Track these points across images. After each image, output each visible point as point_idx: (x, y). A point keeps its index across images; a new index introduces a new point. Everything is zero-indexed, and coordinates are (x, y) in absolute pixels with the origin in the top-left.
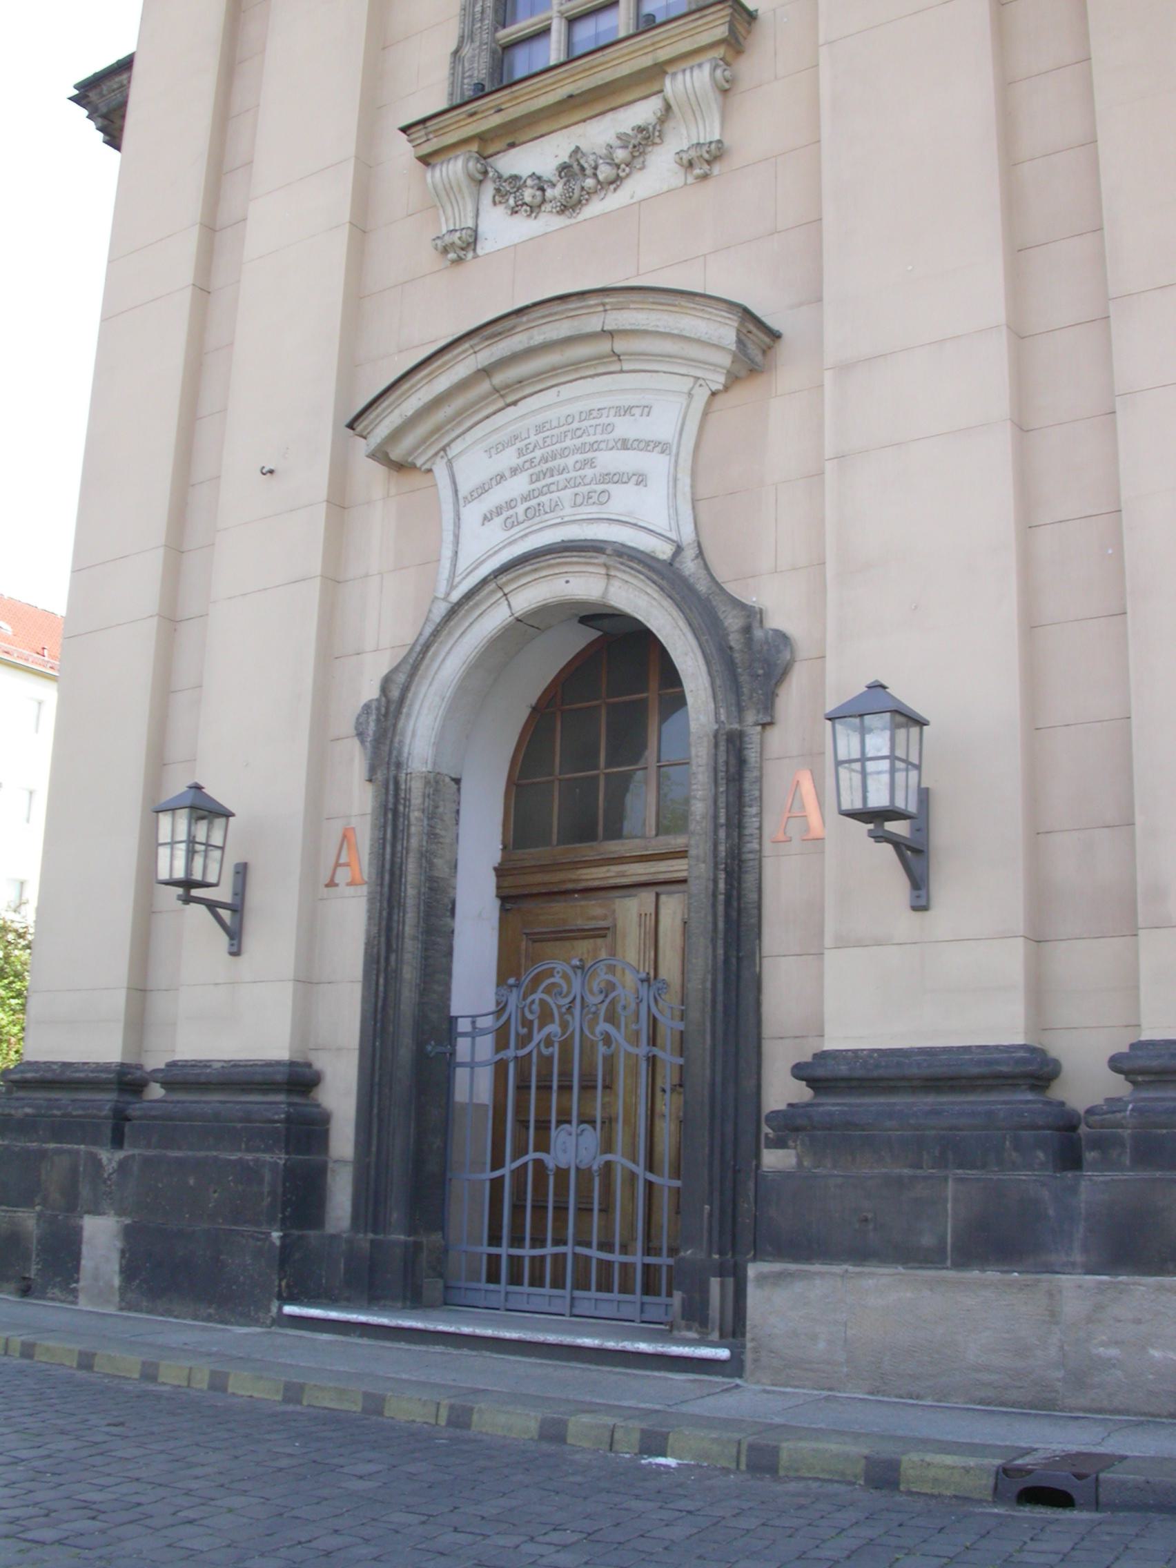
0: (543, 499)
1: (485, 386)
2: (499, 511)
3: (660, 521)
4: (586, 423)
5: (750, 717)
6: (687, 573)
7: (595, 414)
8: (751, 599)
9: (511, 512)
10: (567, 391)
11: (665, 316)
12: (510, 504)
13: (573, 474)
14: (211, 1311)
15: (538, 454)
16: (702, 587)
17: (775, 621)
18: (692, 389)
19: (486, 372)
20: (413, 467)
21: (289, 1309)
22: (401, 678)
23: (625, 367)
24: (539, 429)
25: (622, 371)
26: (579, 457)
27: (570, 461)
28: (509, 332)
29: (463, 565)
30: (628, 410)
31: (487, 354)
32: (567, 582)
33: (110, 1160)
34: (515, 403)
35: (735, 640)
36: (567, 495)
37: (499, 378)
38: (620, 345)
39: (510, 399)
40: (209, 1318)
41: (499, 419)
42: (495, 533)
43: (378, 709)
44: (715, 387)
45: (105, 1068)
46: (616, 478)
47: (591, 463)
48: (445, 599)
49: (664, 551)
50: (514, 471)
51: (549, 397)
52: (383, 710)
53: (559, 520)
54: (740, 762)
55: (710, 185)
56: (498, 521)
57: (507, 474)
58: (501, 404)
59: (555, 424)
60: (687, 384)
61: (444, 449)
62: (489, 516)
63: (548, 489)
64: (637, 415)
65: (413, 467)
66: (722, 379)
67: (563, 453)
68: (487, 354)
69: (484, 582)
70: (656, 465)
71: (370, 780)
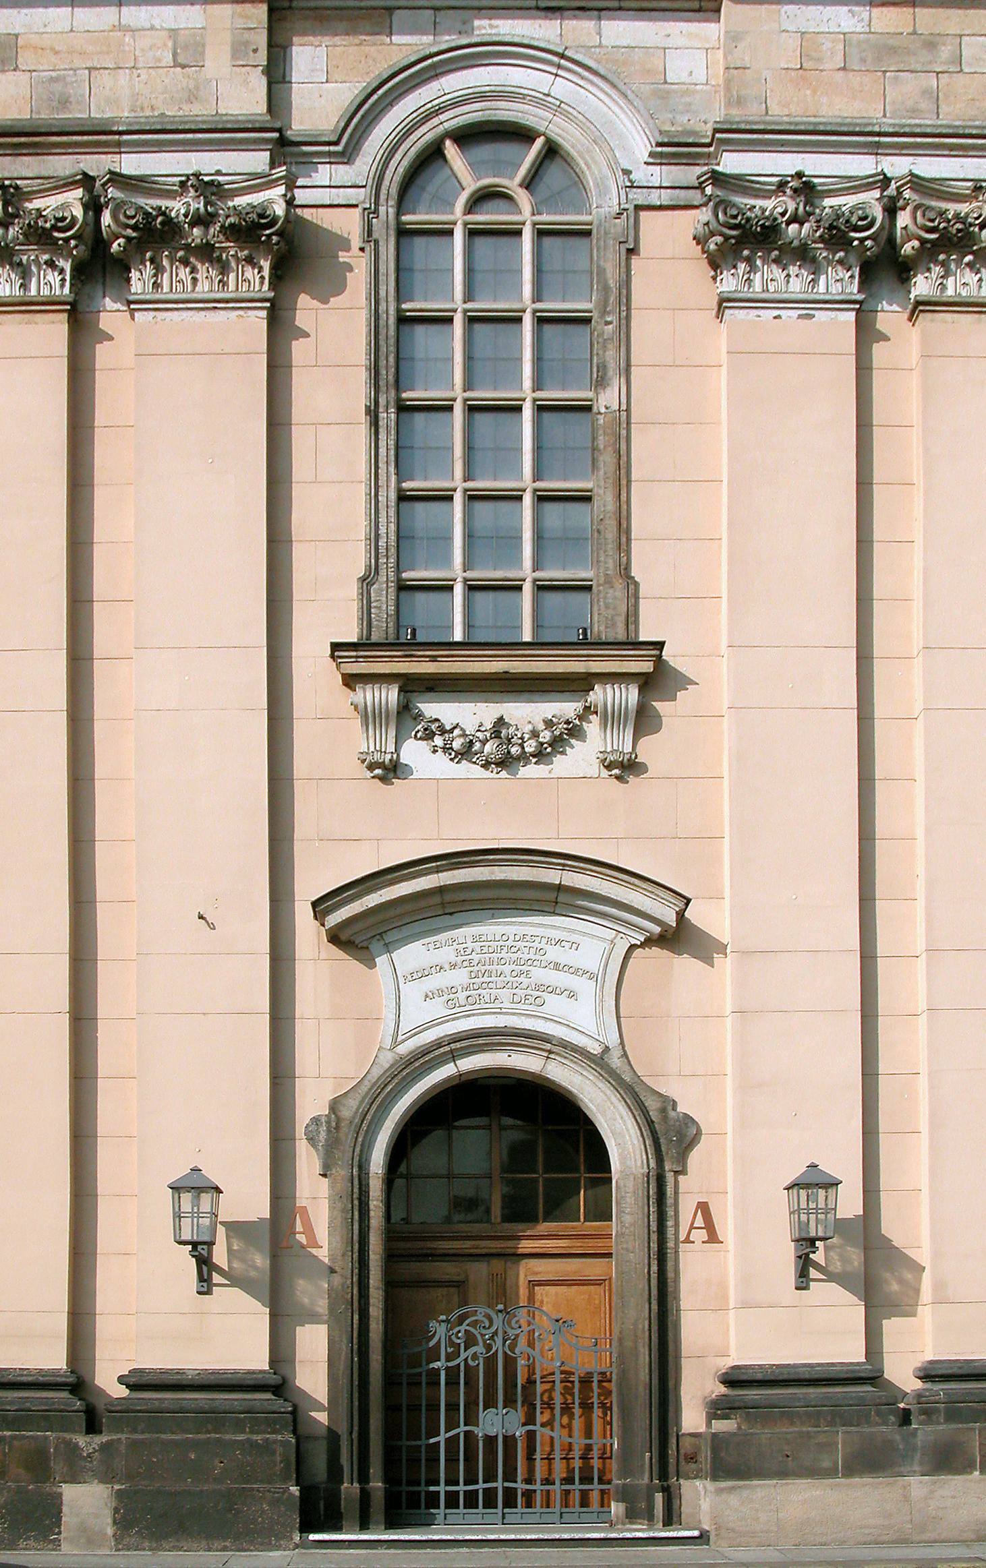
2: (440, 992)
3: (590, 1026)
6: (614, 1066)
7: (528, 938)
9: (452, 996)
13: (509, 978)
16: (627, 1078)
18: (615, 938)
26: (513, 967)
27: (507, 969)
32: (509, 1056)
35: (654, 1115)
36: (505, 994)
46: (550, 989)
50: (453, 966)
53: (499, 1010)
57: (447, 966)
62: (430, 994)
64: (567, 948)
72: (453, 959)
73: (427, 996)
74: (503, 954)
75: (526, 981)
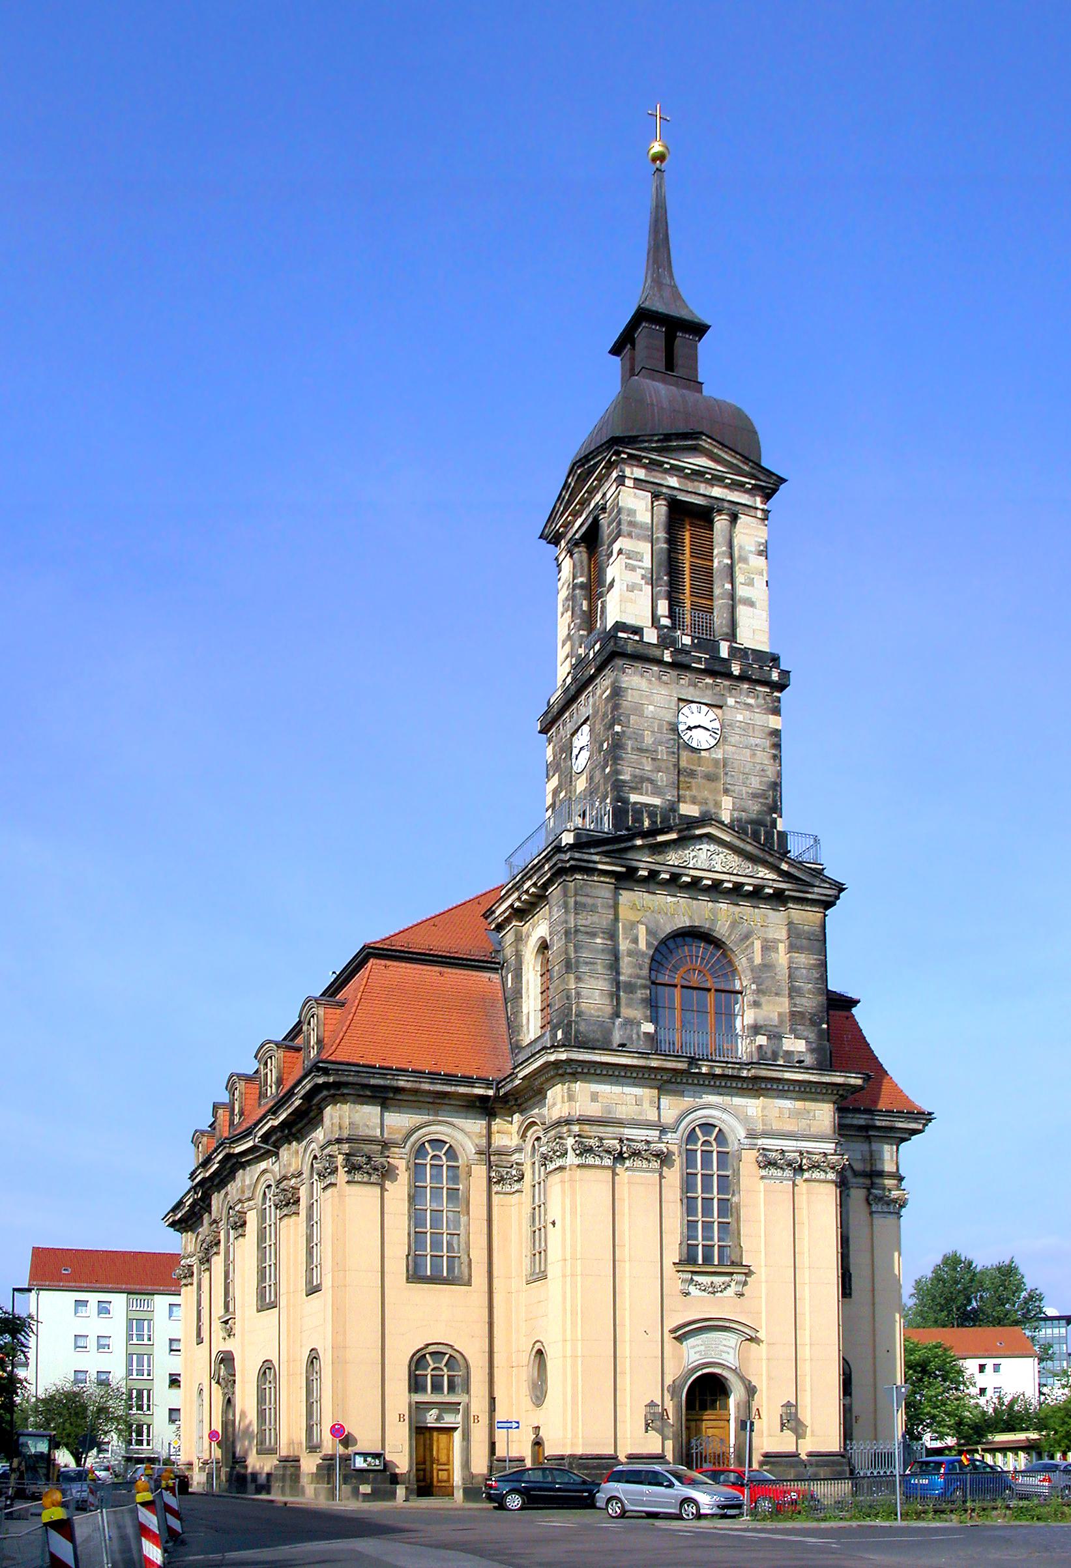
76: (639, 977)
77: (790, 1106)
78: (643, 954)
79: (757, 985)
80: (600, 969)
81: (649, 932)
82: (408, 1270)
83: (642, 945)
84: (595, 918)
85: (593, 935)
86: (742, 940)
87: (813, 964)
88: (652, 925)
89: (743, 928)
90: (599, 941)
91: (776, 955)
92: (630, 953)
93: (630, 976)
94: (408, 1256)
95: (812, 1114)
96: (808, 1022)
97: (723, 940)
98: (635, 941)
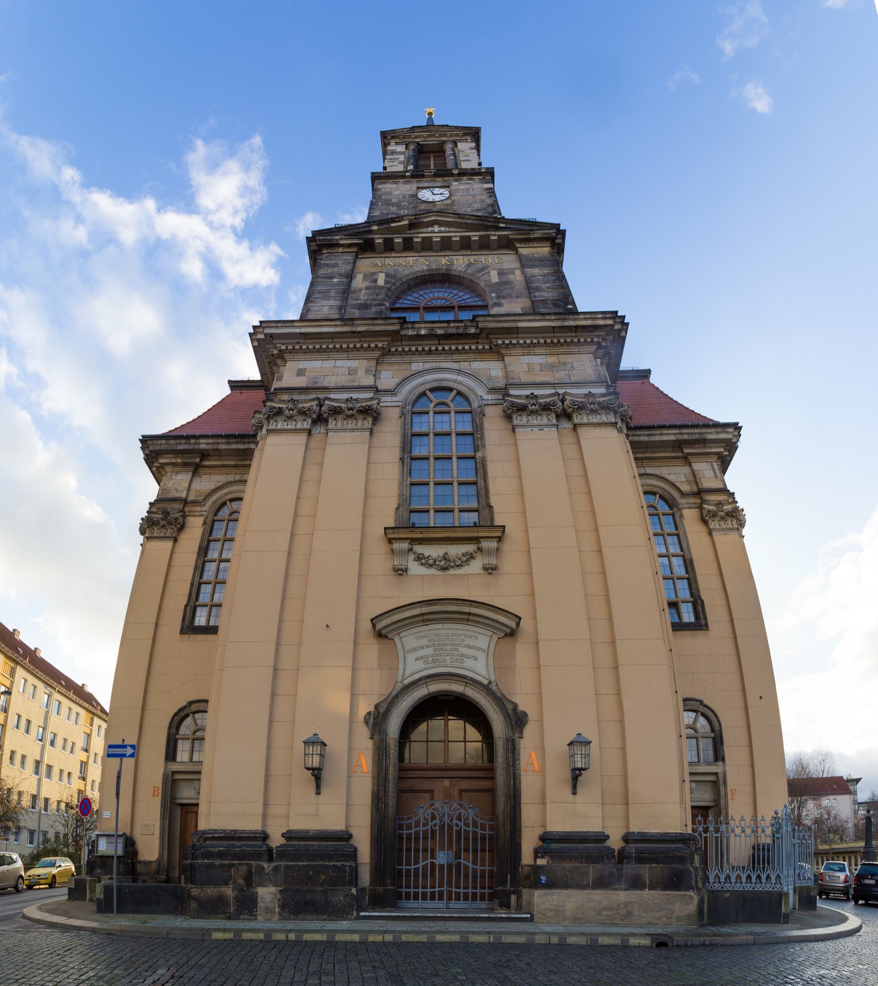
0: (440, 658)
1: (421, 618)
2: (422, 658)
3: (484, 672)
4: (454, 637)
5: (516, 735)
6: (493, 689)
8: (514, 700)
10: (446, 626)
11: (491, 613)
12: (427, 656)
14: (326, 917)
15: (436, 642)
16: (499, 695)
17: (521, 708)
19: (422, 615)
20: (386, 637)
21: (362, 914)
22: (385, 706)
23: (469, 623)
24: (436, 635)
25: (468, 624)
26: (451, 647)
27: (449, 648)
28: (435, 604)
29: (408, 672)
30: (470, 637)
31: (425, 610)
33: (268, 867)
34: (427, 625)
35: (510, 711)
37: (425, 617)
38: (471, 617)
39: (425, 624)
40: (324, 920)
41: (421, 629)
42: (420, 665)
43: (374, 714)
44: (500, 636)
45: (256, 832)
47: (457, 650)
48: (401, 682)
49: (486, 682)
50: (428, 646)
51: (440, 626)
52: (376, 715)
54: (514, 747)
55: (492, 576)
56: (421, 662)
57: (424, 647)
58: (422, 624)
59: (442, 635)
60: (490, 633)
61: (398, 633)
63: (440, 655)
65: (386, 637)
66: (503, 635)
67: (446, 645)
68: (425, 610)
69: (420, 679)
70: (482, 656)
71: (371, 738)
72: (427, 643)
73: (416, 659)
74: (447, 642)
75: (456, 653)
76: (374, 300)
77: (540, 361)
78: (380, 288)
79: (496, 293)
80: (332, 294)
81: (387, 275)
82: (183, 621)
83: (381, 282)
84: (335, 270)
85: (332, 278)
86: (477, 272)
87: (549, 273)
88: (392, 272)
89: (480, 266)
90: (335, 280)
91: (513, 276)
92: (367, 288)
93: (367, 300)
94: (186, 606)
95: (569, 366)
96: (551, 306)
97: (462, 275)
98: (376, 281)
